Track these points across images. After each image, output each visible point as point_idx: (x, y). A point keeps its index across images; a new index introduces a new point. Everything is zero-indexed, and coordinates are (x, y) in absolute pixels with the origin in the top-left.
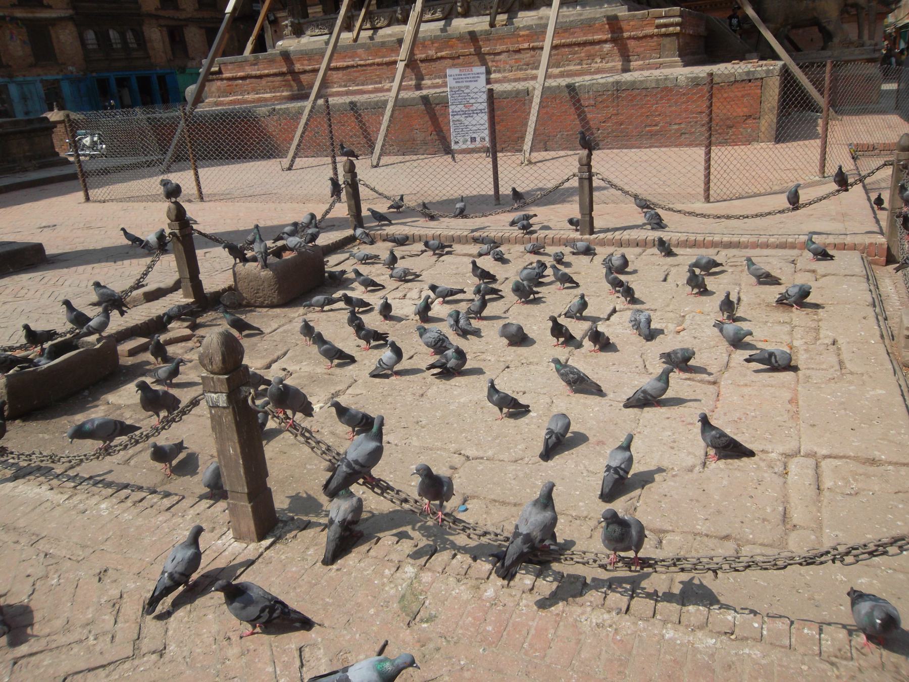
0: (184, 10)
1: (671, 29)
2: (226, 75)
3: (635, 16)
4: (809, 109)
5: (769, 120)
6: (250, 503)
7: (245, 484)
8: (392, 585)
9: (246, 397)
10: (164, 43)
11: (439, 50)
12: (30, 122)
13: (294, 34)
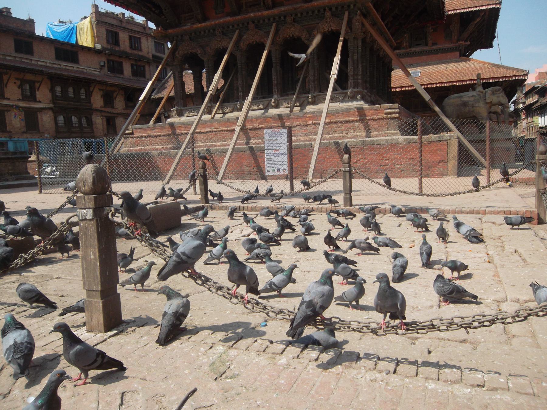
0: (117, 108)
1: (394, 115)
2: (136, 135)
3: (373, 108)
4: (474, 164)
5: (452, 164)
6: (101, 299)
7: (99, 283)
8: (205, 357)
9: (108, 214)
10: (103, 125)
11: (260, 124)
12: (15, 153)
13: (178, 115)
